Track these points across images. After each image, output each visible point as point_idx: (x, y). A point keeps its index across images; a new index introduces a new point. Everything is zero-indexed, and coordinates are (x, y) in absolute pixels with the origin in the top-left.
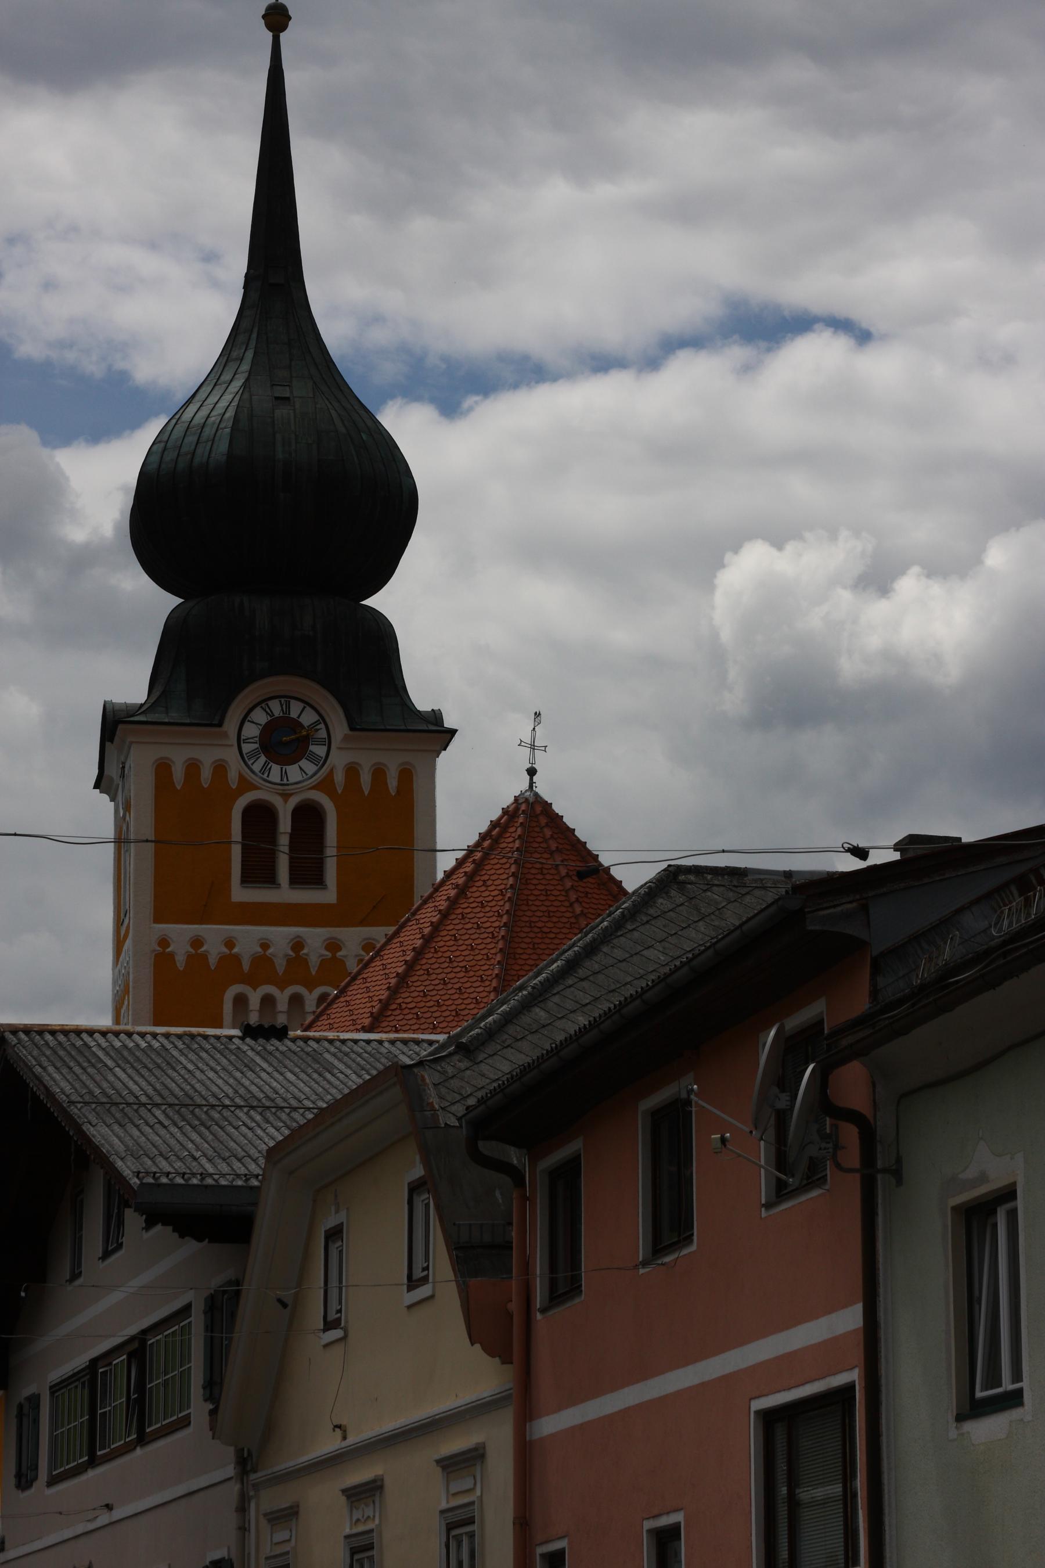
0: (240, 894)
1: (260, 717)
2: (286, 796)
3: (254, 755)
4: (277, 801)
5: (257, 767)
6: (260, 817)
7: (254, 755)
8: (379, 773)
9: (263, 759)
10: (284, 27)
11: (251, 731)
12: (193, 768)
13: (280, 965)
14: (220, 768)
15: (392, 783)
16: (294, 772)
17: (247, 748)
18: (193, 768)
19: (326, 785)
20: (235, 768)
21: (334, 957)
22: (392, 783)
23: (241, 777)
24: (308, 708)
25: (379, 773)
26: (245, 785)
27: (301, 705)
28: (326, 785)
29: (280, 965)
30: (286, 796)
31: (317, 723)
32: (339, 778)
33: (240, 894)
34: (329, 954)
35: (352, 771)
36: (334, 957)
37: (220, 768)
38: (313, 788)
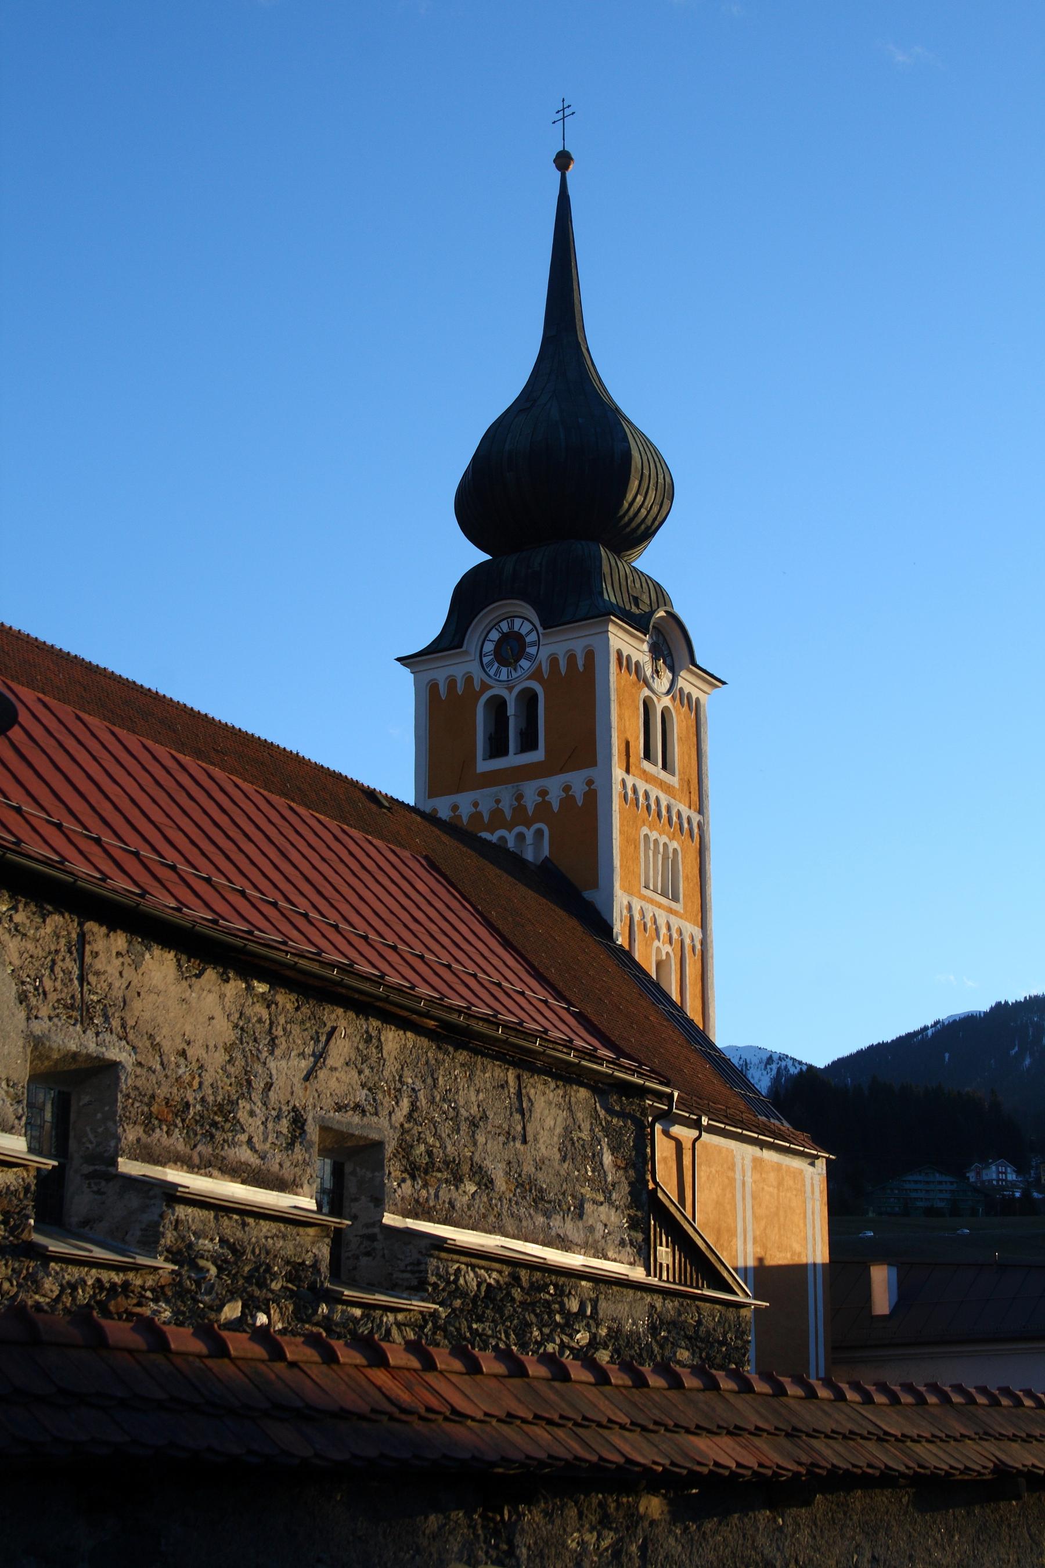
0: (484, 766)
1: (495, 635)
2: (510, 689)
3: (490, 664)
4: (505, 693)
5: (492, 673)
8: (572, 658)
9: (496, 665)
10: (567, 167)
11: (489, 647)
12: (452, 683)
13: (508, 814)
14: (469, 680)
15: (580, 663)
17: (486, 660)
18: (452, 683)
19: (537, 675)
20: (478, 675)
21: (544, 800)
22: (580, 663)
25: (572, 658)
26: (485, 687)
28: (537, 675)
29: (508, 814)
30: (510, 689)
31: (531, 631)
32: (546, 668)
33: (484, 766)
34: (540, 799)
35: (554, 661)
36: (544, 800)
37: (469, 680)
38: (527, 679)
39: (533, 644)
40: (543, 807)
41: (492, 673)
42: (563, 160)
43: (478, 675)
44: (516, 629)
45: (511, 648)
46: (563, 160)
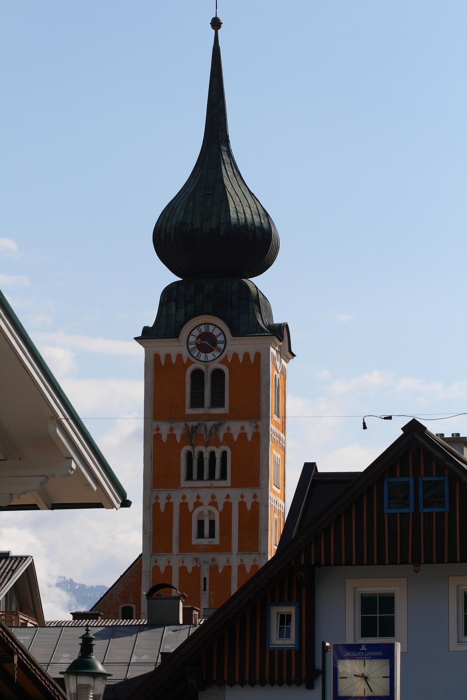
6: (198, 376)
7: (194, 348)
11: (192, 339)
12: (168, 357)
14: (179, 356)
16: (210, 356)
17: (191, 347)
18: (168, 357)
20: (186, 355)
23: (188, 359)
24: (216, 328)
26: (190, 362)
27: (214, 327)
28: (224, 362)
37: (179, 356)
39: (221, 342)
40: (228, 436)
41: (195, 355)
42: (216, 24)
43: (186, 355)
44: (210, 331)
45: (207, 343)
46: (216, 24)
